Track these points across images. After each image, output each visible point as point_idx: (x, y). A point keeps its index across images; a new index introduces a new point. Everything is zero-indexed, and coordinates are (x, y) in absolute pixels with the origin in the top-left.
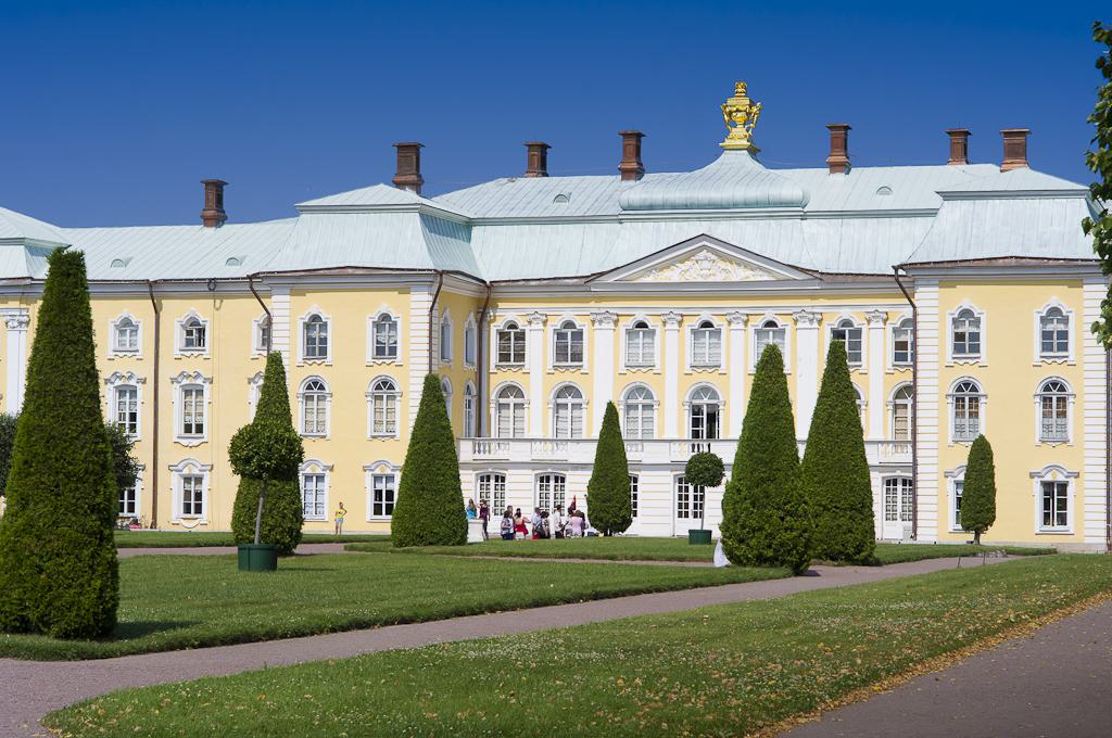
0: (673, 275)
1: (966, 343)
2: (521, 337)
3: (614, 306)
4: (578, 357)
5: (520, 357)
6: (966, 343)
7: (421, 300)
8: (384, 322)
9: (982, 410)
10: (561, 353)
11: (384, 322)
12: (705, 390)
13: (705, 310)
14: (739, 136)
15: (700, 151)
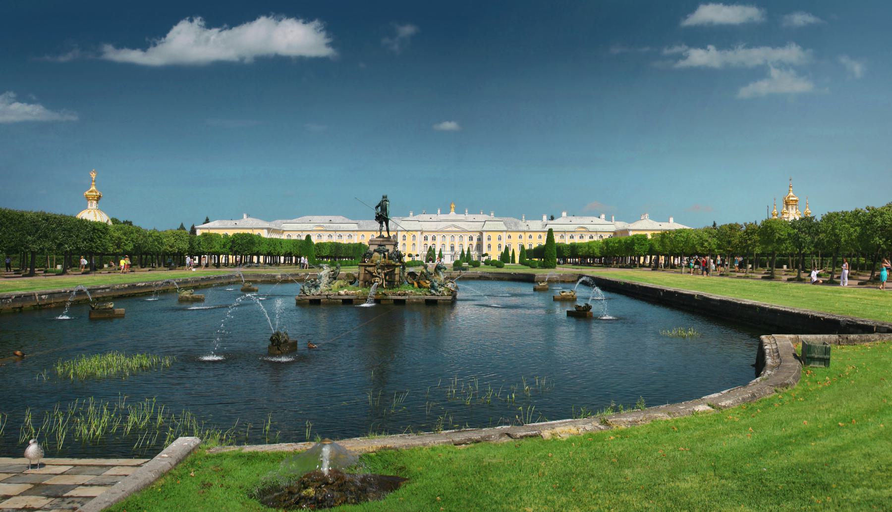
0: (448, 229)
1: (489, 239)
2: (427, 237)
3: (440, 233)
4: (435, 240)
5: (427, 240)
6: (489, 239)
7: (419, 233)
8: (414, 236)
9: (491, 247)
10: (433, 239)
11: (414, 236)
12: (452, 244)
13: (453, 234)
14: (453, 209)
15: (448, 212)
